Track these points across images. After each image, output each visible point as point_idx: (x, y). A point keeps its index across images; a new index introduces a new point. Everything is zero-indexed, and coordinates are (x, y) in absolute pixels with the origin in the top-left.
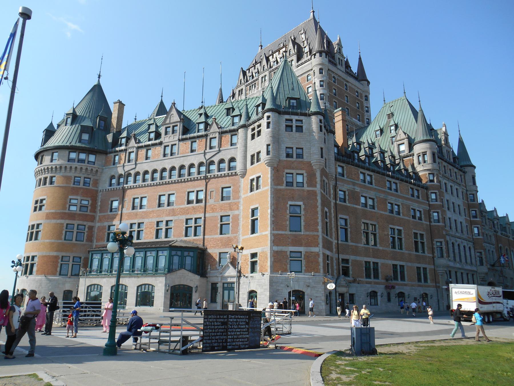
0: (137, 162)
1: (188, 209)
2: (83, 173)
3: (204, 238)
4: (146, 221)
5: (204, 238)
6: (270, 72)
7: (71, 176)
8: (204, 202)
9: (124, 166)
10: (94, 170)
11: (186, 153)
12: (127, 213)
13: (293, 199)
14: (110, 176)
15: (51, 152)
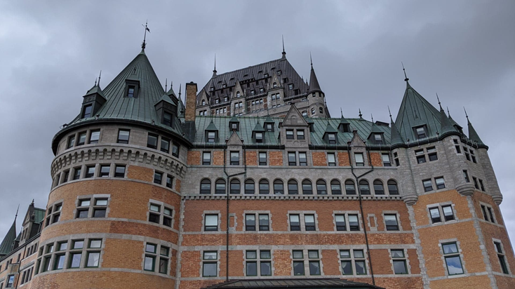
0: (248, 166)
1: (340, 236)
2: (167, 167)
3: (373, 277)
4: (273, 248)
5: (373, 277)
6: (247, 100)
7: (152, 170)
8: (362, 229)
9: (225, 168)
10: (180, 166)
11: (323, 165)
12: (237, 235)
13: (493, 235)
14: (201, 178)
15: (116, 128)
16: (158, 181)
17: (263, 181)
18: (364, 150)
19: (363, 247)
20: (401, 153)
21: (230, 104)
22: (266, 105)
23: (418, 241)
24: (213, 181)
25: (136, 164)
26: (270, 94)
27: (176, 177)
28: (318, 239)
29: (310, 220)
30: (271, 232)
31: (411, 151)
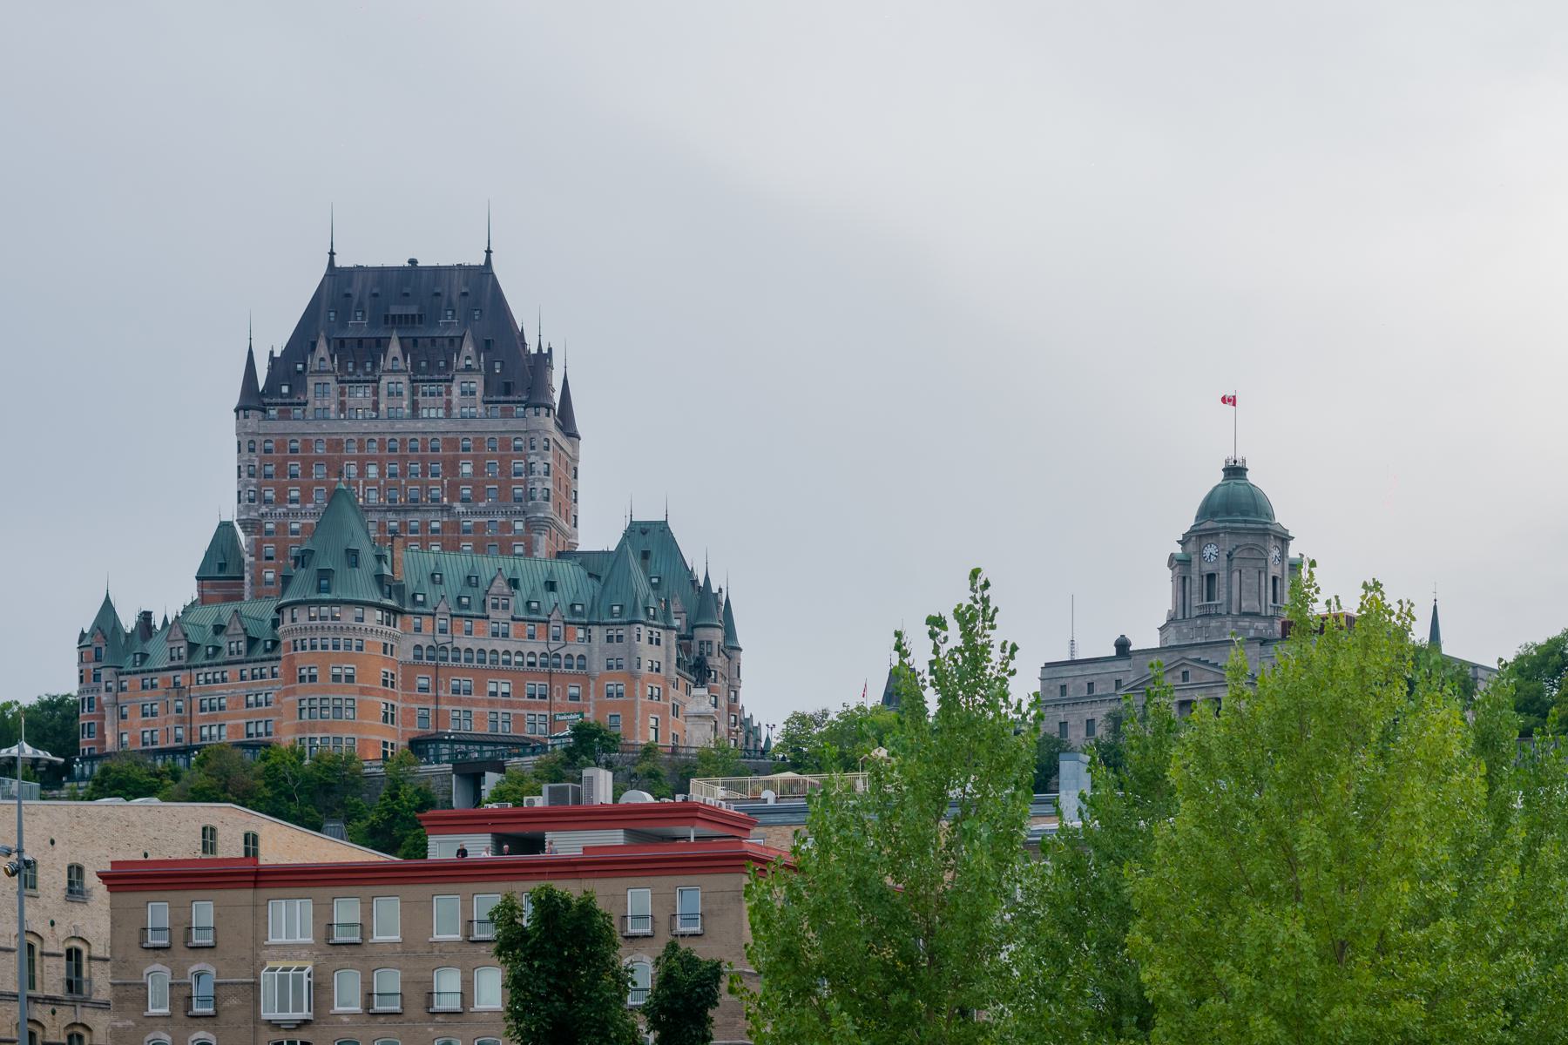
1: (530, 703)
4: (474, 710)
6: (413, 381)
13: (653, 712)
16: (385, 652)
17: (469, 650)
18: (562, 625)
19: (547, 713)
20: (596, 630)
21: (377, 382)
22: (449, 402)
23: (592, 711)
24: (425, 648)
25: (370, 639)
26: (458, 378)
27: (395, 645)
28: (511, 705)
29: (505, 688)
30: (473, 696)
31: (604, 629)
